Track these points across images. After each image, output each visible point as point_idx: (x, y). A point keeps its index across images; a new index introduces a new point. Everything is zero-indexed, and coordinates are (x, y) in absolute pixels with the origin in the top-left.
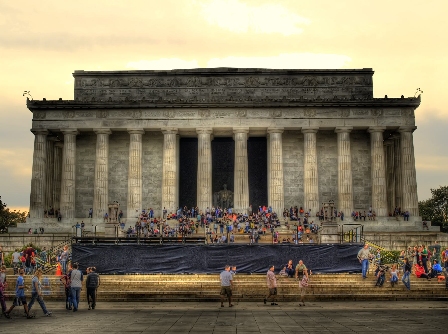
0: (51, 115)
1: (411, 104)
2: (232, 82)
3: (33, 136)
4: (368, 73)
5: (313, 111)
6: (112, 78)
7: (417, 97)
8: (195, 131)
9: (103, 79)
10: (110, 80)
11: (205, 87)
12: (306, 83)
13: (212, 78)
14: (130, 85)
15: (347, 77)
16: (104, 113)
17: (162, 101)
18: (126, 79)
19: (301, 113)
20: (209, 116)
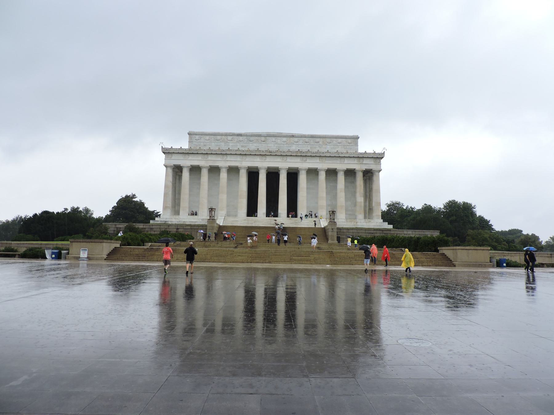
0: (174, 156)
2: (279, 141)
3: (165, 168)
8: (257, 168)
13: (268, 138)
15: (344, 140)
16: (206, 156)
18: (219, 137)
19: (317, 160)
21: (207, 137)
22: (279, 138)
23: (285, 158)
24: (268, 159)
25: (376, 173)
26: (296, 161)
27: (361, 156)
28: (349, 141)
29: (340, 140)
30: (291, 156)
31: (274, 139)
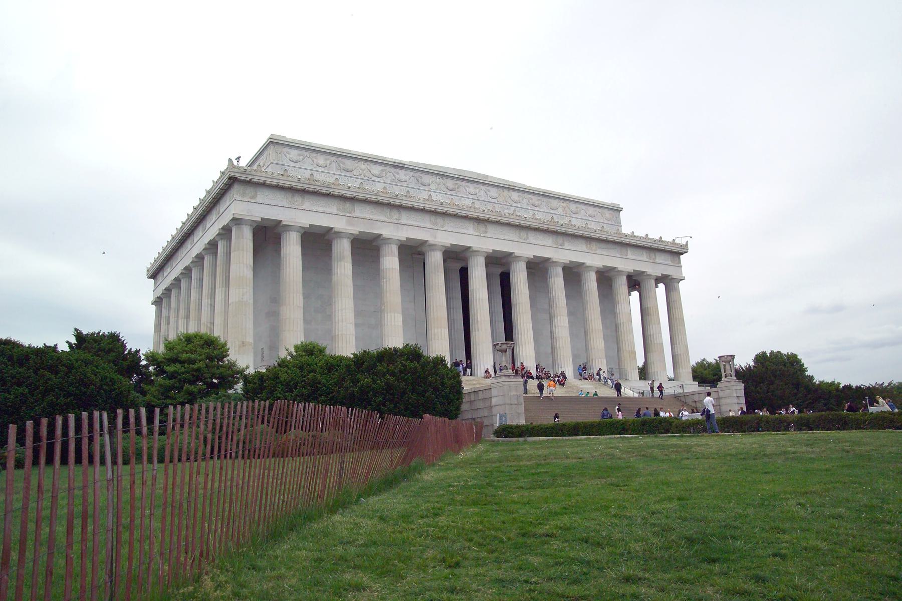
1: (681, 250)
2: (482, 193)
4: (616, 210)
5: (594, 245)
6: (328, 157)
7: (684, 243)
9: (315, 155)
10: (326, 160)
11: (452, 193)
12: (560, 210)
13: (459, 183)
14: (355, 172)
15: (598, 210)
16: (348, 205)
17: (432, 201)
18: (349, 164)
19: (582, 246)
20: (486, 232)
21: (321, 160)
22: (483, 187)
23: (523, 234)
24: (492, 230)
25: (676, 284)
26: (545, 243)
27: (655, 246)
28: (608, 214)
29: (591, 210)
30: (537, 230)
31: (471, 188)
